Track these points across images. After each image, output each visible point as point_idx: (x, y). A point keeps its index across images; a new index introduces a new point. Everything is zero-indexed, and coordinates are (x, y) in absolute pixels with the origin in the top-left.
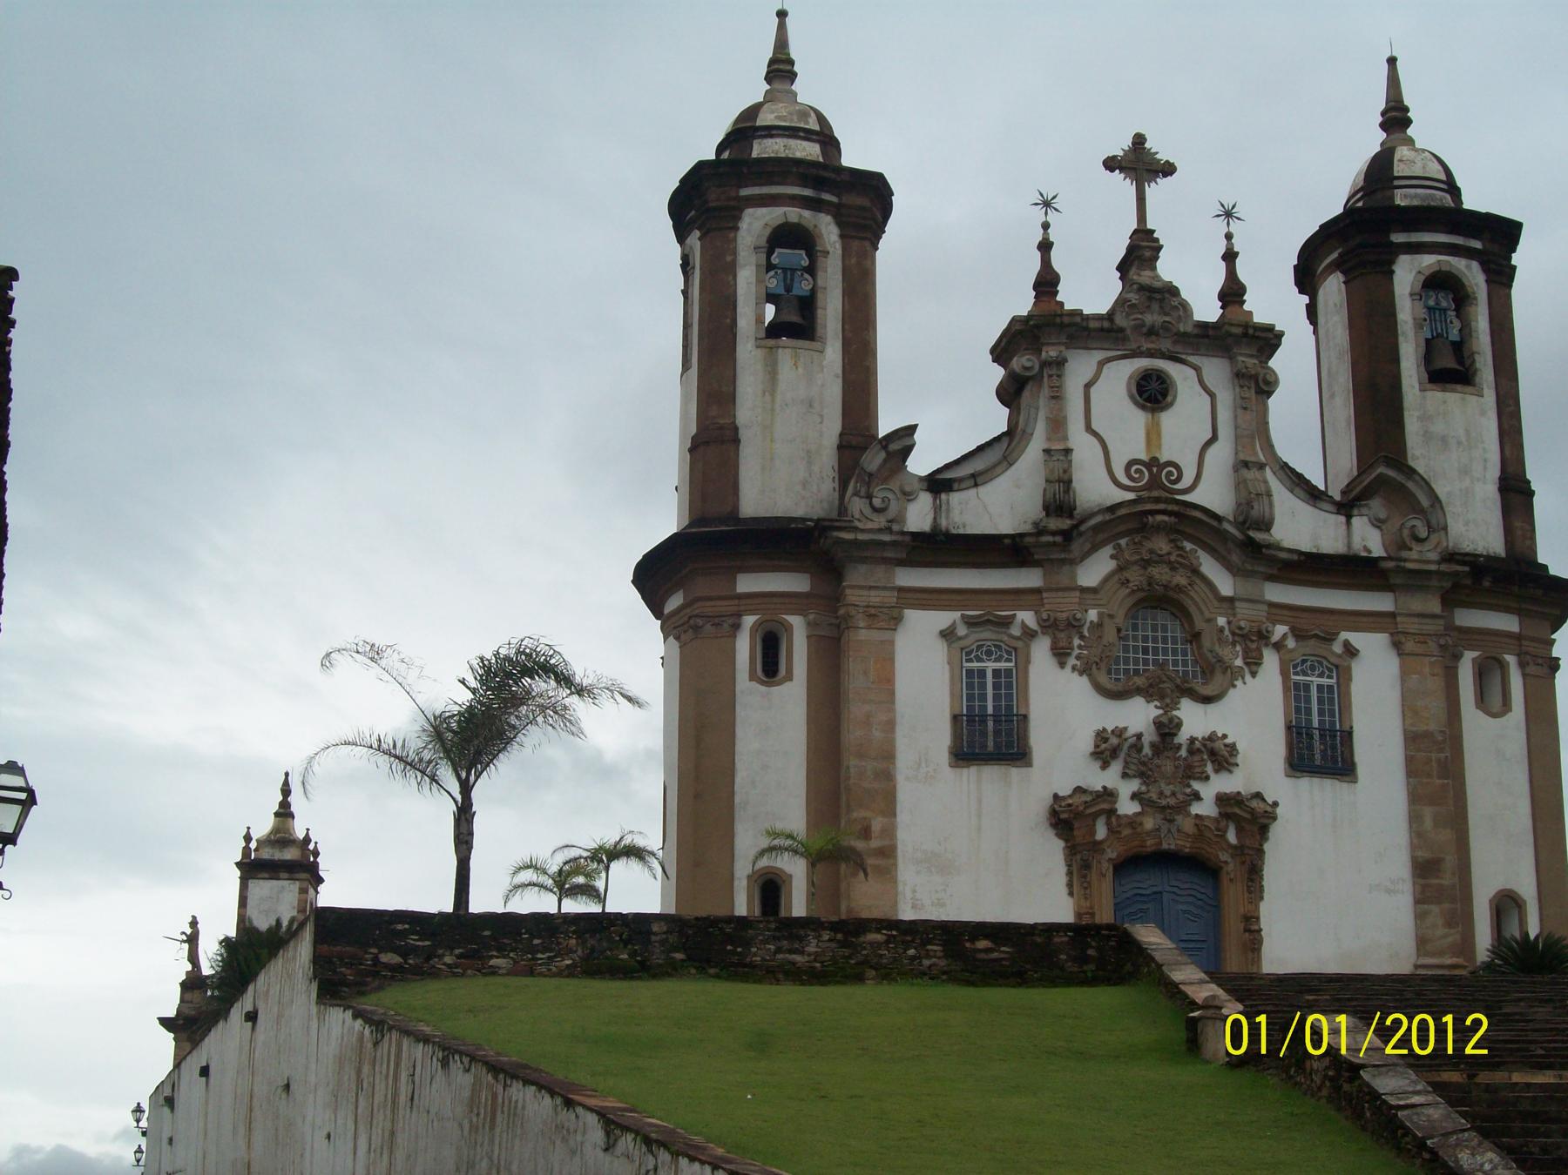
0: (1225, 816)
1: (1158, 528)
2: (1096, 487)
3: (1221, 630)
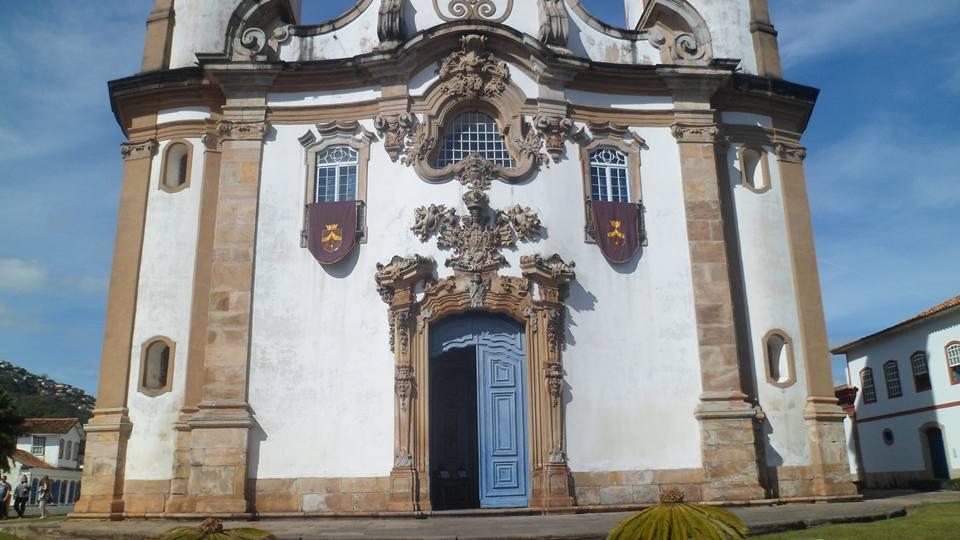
0: (526, 275)
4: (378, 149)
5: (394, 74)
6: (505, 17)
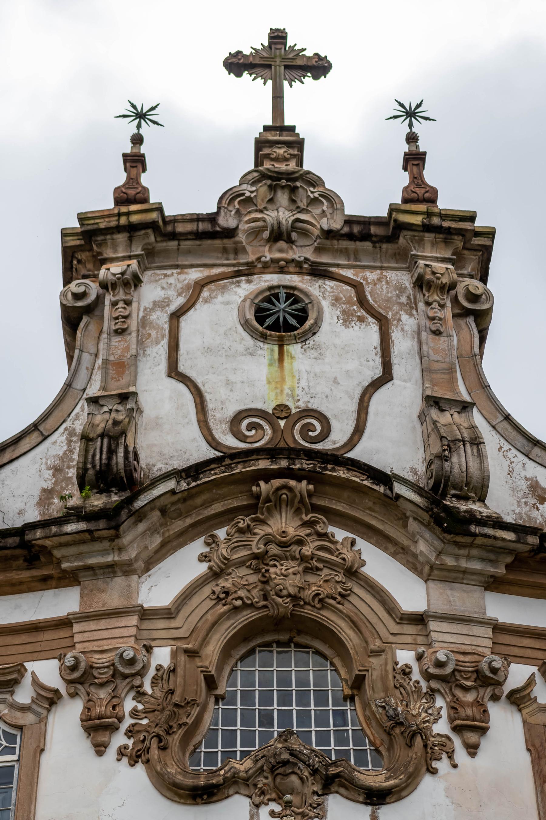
1: (275, 503)
2: (168, 436)
3: (406, 672)
4: (67, 719)
5: (109, 559)
6: (352, 443)
